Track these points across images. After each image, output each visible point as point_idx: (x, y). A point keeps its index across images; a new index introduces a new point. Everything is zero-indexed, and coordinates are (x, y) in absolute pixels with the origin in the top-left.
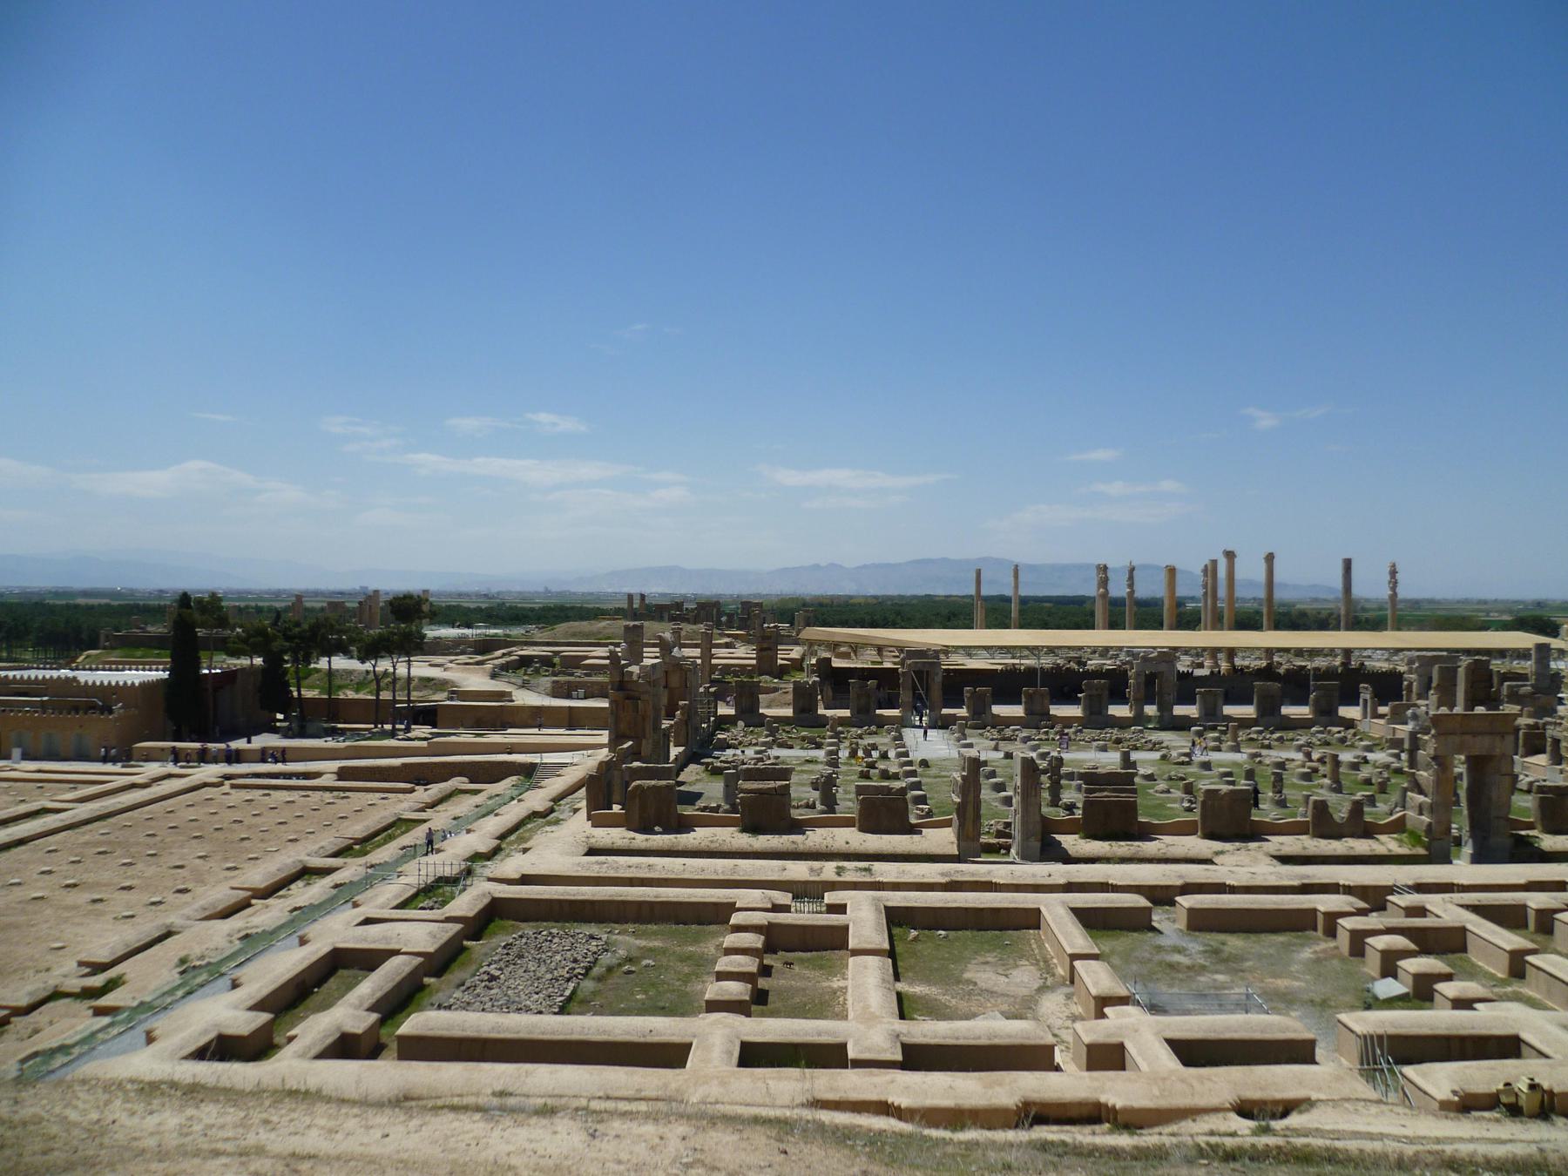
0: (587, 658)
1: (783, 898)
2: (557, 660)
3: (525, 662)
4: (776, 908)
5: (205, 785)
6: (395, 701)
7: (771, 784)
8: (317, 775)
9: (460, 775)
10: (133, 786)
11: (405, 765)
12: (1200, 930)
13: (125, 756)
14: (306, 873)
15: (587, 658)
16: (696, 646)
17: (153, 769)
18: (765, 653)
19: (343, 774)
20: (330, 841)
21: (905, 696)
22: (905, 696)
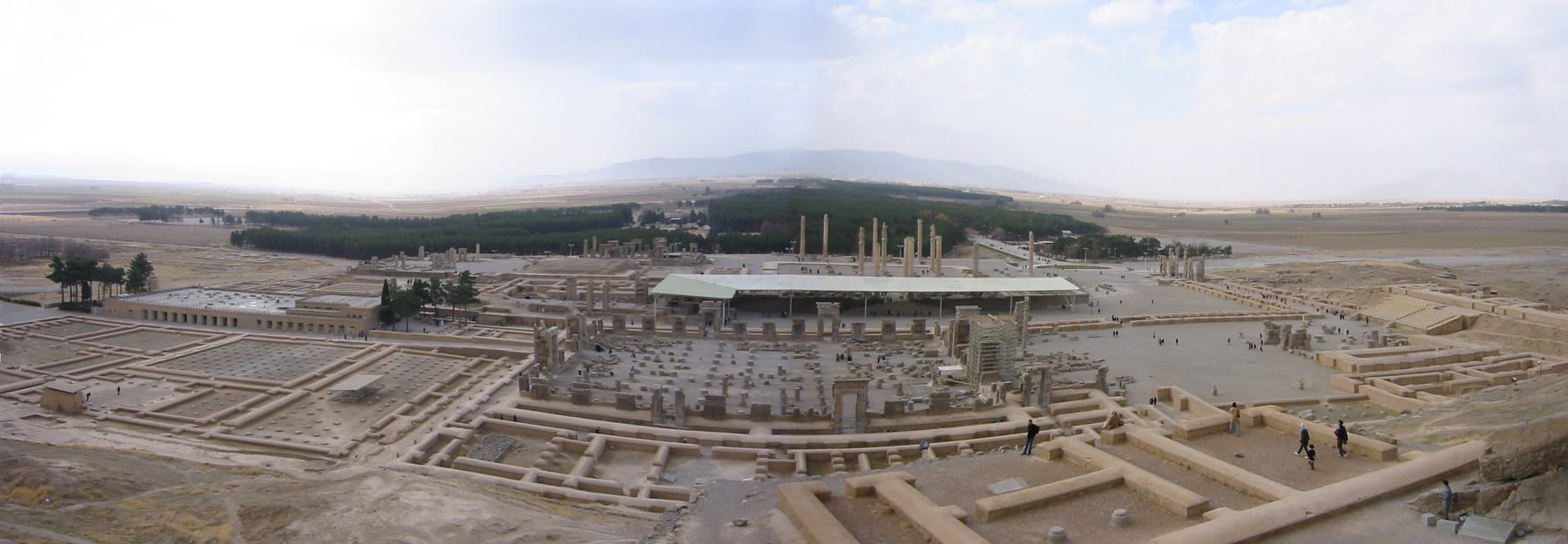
0: (550, 288)
2: (535, 286)
3: (520, 289)
4: (571, 437)
7: (582, 390)
15: (550, 288)
21: (702, 324)
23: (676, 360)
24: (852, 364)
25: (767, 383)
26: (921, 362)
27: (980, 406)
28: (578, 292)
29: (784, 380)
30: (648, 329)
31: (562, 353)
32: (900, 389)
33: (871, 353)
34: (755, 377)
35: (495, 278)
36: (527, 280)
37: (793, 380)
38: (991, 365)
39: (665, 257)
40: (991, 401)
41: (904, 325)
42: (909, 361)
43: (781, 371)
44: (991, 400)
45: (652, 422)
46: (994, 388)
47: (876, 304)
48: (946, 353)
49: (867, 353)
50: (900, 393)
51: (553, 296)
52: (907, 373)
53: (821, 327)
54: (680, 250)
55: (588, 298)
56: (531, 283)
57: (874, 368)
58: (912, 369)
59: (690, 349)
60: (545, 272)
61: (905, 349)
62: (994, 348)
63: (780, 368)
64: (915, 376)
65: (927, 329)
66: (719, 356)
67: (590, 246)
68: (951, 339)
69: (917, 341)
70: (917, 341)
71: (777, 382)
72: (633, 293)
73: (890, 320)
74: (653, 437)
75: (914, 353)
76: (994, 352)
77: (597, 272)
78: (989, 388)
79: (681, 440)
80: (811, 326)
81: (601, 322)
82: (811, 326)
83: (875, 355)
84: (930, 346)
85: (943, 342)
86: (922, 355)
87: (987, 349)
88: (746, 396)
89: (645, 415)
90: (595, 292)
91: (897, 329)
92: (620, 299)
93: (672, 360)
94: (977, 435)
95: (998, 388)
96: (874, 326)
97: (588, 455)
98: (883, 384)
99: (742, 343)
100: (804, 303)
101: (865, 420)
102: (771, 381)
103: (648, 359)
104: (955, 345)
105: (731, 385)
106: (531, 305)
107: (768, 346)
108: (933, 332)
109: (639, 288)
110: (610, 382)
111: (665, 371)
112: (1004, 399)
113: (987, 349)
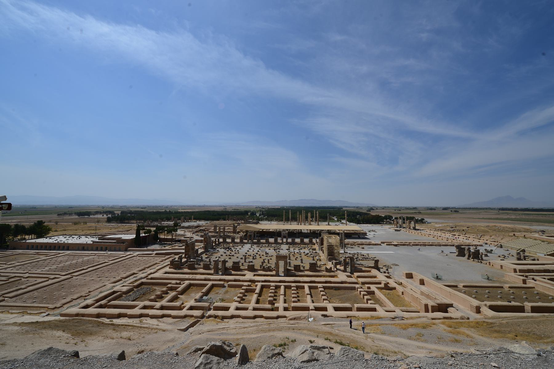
0: (210, 230)
1: (178, 282)
5: (134, 256)
6: (176, 238)
8: (153, 254)
9: (173, 254)
10: (123, 257)
11: (165, 253)
12: (229, 287)
13: (126, 250)
14: (134, 274)
16: (232, 226)
17: (128, 253)
19: (156, 254)
20: (140, 268)
22: (248, 239)
23: (236, 250)
24: (289, 251)
25: (261, 257)
26: (310, 252)
27: (327, 270)
28: (217, 230)
29: (267, 256)
30: (233, 241)
31: (197, 250)
32: (302, 260)
35: (194, 227)
36: (205, 227)
37: (269, 256)
38: (331, 254)
39: (247, 221)
40: (331, 268)
41: (306, 240)
42: (307, 251)
43: (266, 253)
44: (331, 268)
45: (213, 274)
46: (333, 264)
48: (318, 249)
49: (295, 248)
50: (302, 262)
51: (210, 232)
52: (305, 255)
53: (282, 240)
54: (252, 220)
55: (219, 233)
56: (206, 228)
57: (296, 253)
58: (308, 254)
59: (242, 247)
60: (211, 225)
61: (306, 247)
62: (331, 247)
63: (266, 252)
64: (308, 256)
66: (250, 249)
67: (228, 217)
68: (319, 244)
69: (310, 245)
72: (232, 230)
73: (303, 238)
74: (209, 280)
75: (309, 249)
76: (332, 249)
77: (221, 225)
79: (220, 280)
80: (279, 240)
81: (219, 240)
82: (279, 240)
83: (297, 249)
84: (314, 247)
86: (311, 250)
87: (330, 247)
88: (252, 262)
89: (212, 272)
90: (221, 230)
92: (229, 232)
94: (326, 282)
95: (334, 263)
96: (298, 240)
97: (177, 292)
98: (297, 259)
100: (276, 234)
101: (288, 273)
102: (262, 257)
104: (321, 246)
105: (249, 258)
106: (201, 235)
107: (266, 246)
108: (315, 243)
109: (234, 229)
110: (208, 260)
111: (230, 254)
112: (336, 267)
113: (330, 247)
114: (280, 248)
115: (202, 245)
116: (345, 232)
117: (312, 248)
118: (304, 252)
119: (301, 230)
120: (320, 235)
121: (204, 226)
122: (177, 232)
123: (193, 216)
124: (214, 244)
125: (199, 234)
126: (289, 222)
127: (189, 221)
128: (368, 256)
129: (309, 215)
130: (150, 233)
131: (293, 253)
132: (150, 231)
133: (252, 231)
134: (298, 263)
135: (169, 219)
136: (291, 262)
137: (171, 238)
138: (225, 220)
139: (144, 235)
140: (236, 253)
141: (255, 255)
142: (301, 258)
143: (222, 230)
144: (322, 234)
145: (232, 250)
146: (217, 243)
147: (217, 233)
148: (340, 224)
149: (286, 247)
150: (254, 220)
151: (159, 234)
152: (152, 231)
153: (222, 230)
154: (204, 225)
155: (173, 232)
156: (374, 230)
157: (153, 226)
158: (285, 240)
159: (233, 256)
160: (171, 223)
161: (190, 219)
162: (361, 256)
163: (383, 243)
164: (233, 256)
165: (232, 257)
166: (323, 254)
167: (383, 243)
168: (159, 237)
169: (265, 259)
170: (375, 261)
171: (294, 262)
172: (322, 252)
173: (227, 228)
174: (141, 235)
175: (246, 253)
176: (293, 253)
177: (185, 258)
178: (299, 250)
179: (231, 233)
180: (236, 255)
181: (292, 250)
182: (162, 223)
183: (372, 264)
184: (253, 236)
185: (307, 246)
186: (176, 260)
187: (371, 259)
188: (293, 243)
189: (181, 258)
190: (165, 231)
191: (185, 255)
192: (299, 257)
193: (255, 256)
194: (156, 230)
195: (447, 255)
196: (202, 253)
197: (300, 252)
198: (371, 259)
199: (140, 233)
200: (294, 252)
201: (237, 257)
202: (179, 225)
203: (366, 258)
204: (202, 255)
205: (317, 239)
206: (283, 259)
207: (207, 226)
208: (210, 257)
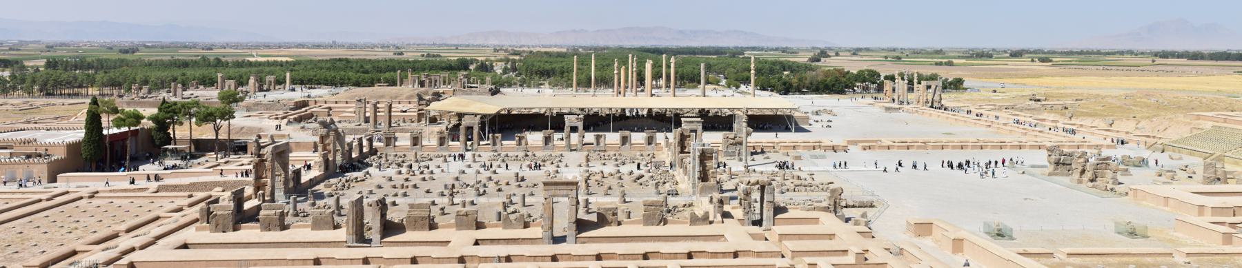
18: (421, 112)
21: (462, 138)
25: (499, 190)
28: (367, 115)
29: (520, 186)
31: (297, 173)
33: (607, 162)
34: (491, 185)
41: (638, 138)
47: (622, 121)
54: (477, 83)
56: (330, 109)
58: (642, 176)
61: (637, 159)
64: (641, 184)
65: (658, 142)
68: (675, 147)
70: (649, 153)
71: (513, 189)
73: (627, 133)
78: (707, 200)
81: (370, 141)
85: (669, 153)
88: (472, 203)
91: (633, 142)
93: (422, 173)
95: (715, 200)
96: (612, 138)
99: (496, 154)
102: (504, 187)
103: (400, 173)
107: (517, 156)
109: (421, 107)
114: (560, 161)
115: (316, 158)
116: (750, 113)
117: (653, 160)
118: (631, 173)
119: (624, 110)
120: (678, 124)
121: (326, 102)
122: (231, 121)
123: (288, 75)
124: (354, 155)
125: (307, 126)
126: (592, 90)
127: (277, 87)
128: (813, 179)
129: (648, 66)
130: (139, 123)
131: (598, 177)
132: (138, 118)
133: (476, 115)
134: (612, 201)
135: (209, 82)
136: (591, 199)
137: (215, 138)
138: (392, 83)
139: (115, 131)
140: (424, 179)
141: (484, 181)
142: (622, 189)
143: (383, 114)
144: (683, 119)
145: (413, 172)
146: (365, 150)
147: (367, 120)
148: (736, 94)
149: (580, 156)
150: (483, 82)
151: (171, 127)
152: (143, 118)
153: (383, 114)
154: (326, 98)
155: (218, 121)
156: (828, 109)
157: (151, 105)
158: (575, 138)
159: (415, 186)
160: (209, 95)
161: (280, 82)
162: (792, 180)
163: (855, 143)
164: (415, 186)
165: (410, 191)
166: (686, 177)
167: (855, 143)
168: (172, 136)
169: (514, 195)
170: (833, 191)
171: (600, 201)
172: (682, 170)
173: (397, 107)
174: (105, 132)
175: (457, 179)
176: (598, 177)
177: (256, 198)
178: (617, 166)
179: (413, 122)
180: (424, 186)
181: (596, 167)
182: (187, 93)
183: (824, 198)
184: (476, 130)
185: (642, 155)
186: (220, 203)
187: (821, 186)
188: (602, 152)
189: (239, 198)
190: (190, 119)
191: (258, 187)
192: (615, 187)
193: (485, 186)
194: (158, 114)
195: (1023, 173)
196: (314, 182)
197: (619, 171)
198: (821, 186)
199: (100, 124)
200: (602, 172)
201: (428, 192)
202: (238, 96)
203: (805, 186)
204: (314, 186)
205: (669, 135)
206: (565, 192)
207: (336, 102)
208: (341, 192)
